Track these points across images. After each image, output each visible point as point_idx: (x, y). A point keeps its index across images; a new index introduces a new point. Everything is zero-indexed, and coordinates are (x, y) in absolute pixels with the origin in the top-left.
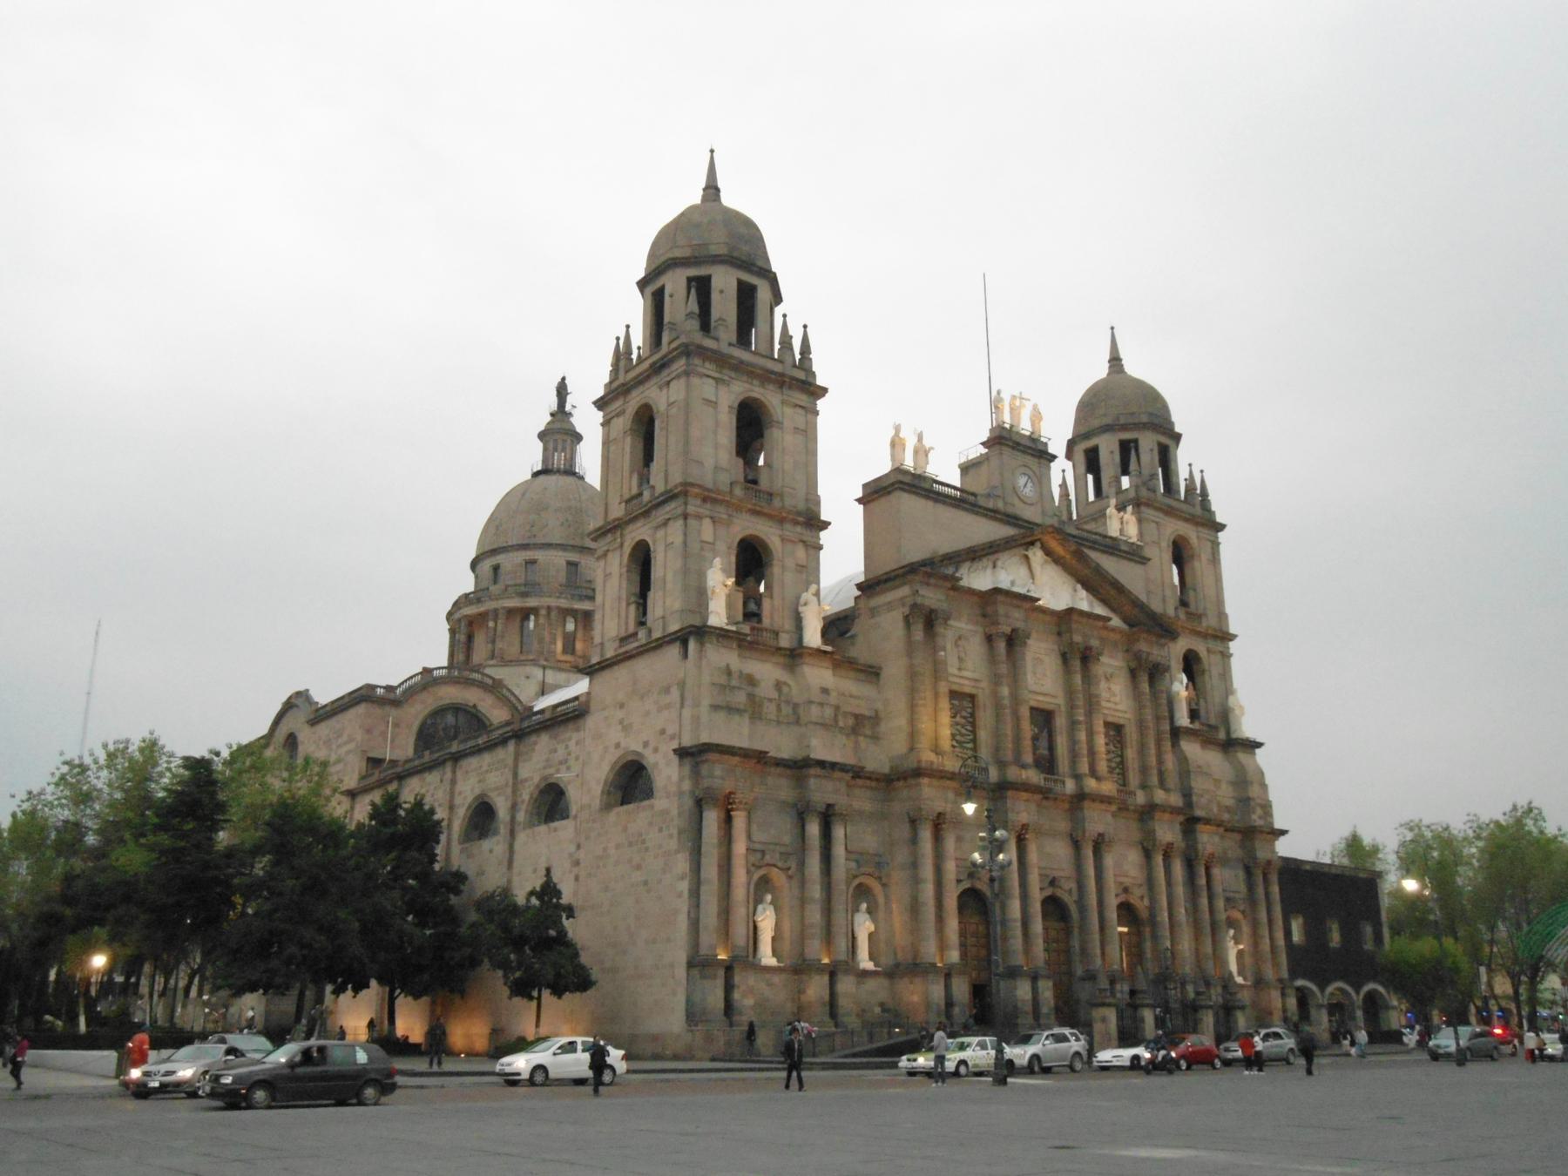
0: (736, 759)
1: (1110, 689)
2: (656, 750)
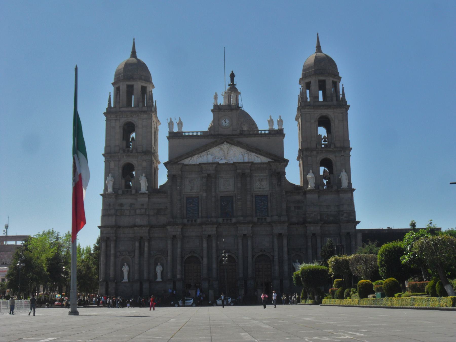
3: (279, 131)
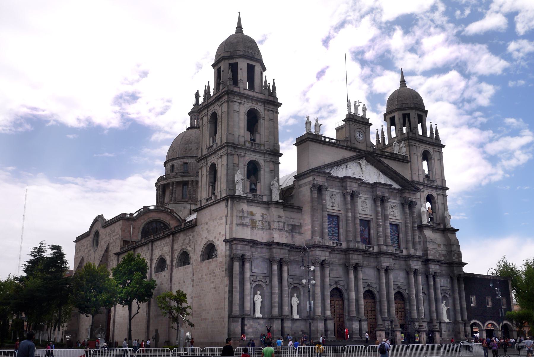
0: (245, 243)
1: (393, 211)
2: (218, 240)
3: (404, 157)
